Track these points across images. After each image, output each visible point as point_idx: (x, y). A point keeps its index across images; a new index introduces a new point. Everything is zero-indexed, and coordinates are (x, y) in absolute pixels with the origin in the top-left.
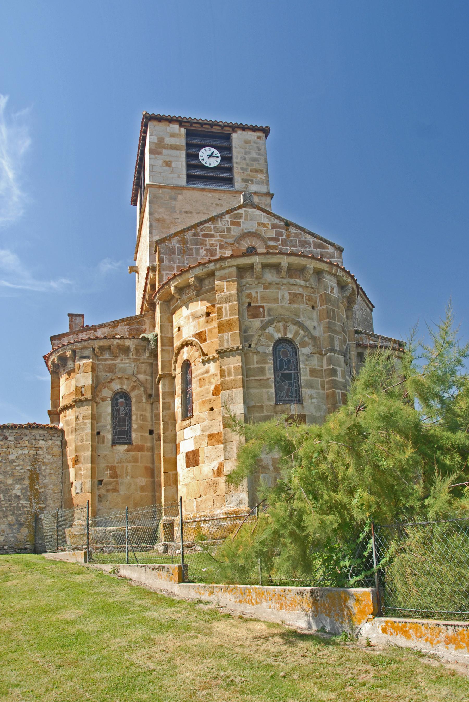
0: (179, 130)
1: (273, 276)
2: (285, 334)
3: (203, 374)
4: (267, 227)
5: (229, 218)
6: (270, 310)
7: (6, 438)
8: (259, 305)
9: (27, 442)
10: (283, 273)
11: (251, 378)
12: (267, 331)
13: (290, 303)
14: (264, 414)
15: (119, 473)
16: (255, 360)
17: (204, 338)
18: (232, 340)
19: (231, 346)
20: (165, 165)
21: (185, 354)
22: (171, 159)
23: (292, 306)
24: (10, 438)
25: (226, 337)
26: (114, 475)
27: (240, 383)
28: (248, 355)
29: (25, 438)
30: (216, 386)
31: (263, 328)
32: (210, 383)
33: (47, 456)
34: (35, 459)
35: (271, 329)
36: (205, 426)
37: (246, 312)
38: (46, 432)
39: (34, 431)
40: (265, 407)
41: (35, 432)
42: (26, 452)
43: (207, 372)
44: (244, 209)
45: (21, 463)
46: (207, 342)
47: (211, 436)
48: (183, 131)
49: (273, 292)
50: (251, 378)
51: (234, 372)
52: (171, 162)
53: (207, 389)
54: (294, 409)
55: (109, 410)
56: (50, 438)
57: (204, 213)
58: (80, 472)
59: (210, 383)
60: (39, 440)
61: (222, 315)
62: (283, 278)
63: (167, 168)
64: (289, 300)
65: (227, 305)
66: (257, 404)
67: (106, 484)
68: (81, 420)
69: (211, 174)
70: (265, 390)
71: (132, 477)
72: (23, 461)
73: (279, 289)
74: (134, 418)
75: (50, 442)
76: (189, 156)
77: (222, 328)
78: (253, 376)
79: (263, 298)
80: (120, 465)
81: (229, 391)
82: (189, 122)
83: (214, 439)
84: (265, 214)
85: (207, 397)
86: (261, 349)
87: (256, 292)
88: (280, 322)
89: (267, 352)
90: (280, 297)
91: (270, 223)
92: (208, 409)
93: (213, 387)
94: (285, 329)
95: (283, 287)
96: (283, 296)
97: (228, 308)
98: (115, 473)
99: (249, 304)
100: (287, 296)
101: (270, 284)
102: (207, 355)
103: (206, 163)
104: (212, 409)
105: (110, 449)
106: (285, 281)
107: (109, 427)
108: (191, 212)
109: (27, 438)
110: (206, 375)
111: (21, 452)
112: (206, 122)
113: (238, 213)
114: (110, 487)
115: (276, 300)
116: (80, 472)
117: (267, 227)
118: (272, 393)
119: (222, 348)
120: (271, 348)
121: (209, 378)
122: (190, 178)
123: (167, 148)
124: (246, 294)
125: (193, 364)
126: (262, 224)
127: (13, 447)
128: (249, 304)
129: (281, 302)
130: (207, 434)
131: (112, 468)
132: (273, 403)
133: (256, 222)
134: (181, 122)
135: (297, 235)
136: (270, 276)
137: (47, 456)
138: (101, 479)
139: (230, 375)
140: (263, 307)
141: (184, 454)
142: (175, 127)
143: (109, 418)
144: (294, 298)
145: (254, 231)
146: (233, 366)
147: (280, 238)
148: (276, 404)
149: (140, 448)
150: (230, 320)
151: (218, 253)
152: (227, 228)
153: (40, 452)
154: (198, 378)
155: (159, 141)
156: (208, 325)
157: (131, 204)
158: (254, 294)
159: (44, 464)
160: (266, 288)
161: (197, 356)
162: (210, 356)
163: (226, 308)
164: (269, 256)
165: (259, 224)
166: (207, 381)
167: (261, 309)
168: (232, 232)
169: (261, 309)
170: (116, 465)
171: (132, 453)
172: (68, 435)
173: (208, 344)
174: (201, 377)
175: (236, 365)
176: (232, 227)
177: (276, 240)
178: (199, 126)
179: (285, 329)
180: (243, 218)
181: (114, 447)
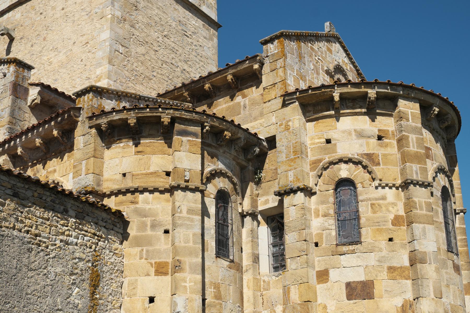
3: (376, 199)
18: (421, 174)
25: (414, 168)
30: (395, 216)
36: (383, 257)
38: (109, 217)
41: (97, 212)
43: (384, 198)
46: (381, 166)
47: (391, 269)
51: (426, 208)
62: (441, 128)
85: (384, 225)
93: (392, 217)
97: (415, 139)
104: (391, 240)
105: (214, 259)
110: (381, 202)
121: (386, 206)
125: (359, 186)
130: (386, 265)
131: (217, 287)
146: (424, 200)
150: (417, 152)
154: (370, 202)
156: (382, 149)
163: (412, 139)
166: (384, 208)
175: (426, 200)
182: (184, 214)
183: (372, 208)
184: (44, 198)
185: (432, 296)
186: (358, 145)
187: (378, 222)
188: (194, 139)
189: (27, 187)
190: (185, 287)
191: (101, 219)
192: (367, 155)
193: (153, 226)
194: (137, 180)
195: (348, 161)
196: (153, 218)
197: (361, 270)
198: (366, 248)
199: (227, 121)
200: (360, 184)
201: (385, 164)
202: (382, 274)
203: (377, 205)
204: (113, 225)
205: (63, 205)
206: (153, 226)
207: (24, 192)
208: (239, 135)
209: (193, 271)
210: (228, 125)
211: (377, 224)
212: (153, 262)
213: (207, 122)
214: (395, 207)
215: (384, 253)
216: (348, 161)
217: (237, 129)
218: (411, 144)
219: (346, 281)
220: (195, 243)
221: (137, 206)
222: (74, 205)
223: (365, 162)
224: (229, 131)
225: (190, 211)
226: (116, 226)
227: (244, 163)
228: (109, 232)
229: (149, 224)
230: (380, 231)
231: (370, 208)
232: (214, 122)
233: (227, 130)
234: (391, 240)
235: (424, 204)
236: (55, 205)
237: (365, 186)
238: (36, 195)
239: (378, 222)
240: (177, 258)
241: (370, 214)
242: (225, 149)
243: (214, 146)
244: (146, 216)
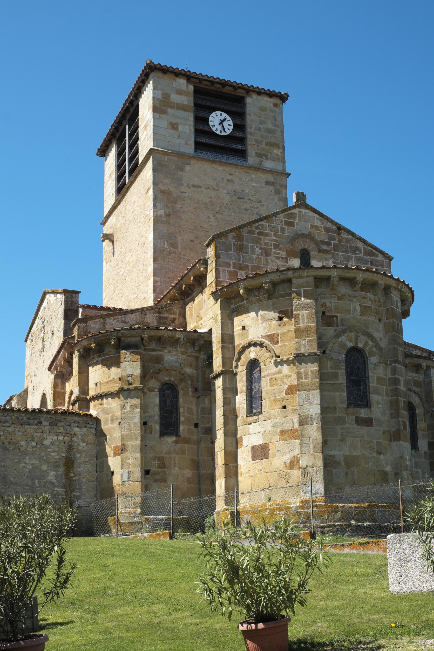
0: (187, 86)
1: (346, 289)
2: (357, 343)
3: (274, 374)
4: (319, 230)
5: (284, 218)
6: (343, 320)
7: (41, 423)
8: (333, 314)
9: (62, 428)
10: (358, 287)
11: (324, 382)
12: (340, 339)
13: (361, 315)
14: (337, 415)
15: (167, 464)
16: (329, 366)
17: (276, 340)
19: (308, 351)
20: (170, 127)
21: (252, 353)
22: (178, 121)
23: (363, 318)
24: (45, 423)
25: (303, 342)
26: (162, 466)
27: (317, 385)
28: (322, 360)
29: (60, 424)
30: (289, 386)
31: (337, 336)
32: (283, 383)
33: (81, 444)
34: (70, 447)
35: (343, 338)
36: (277, 423)
37: (321, 320)
38: (81, 419)
39: (68, 417)
40: (337, 409)
41: (69, 418)
42: (61, 438)
44: (298, 209)
45: (56, 449)
46: (280, 344)
47: (283, 432)
48: (191, 87)
49: (345, 304)
50: (324, 382)
51: (311, 376)
52: (177, 124)
53: (280, 389)
54: (363, 413)
55: (157, 400)
56: (84, 425)
57: (214, 189)
58: (127, 461)
59: (283, 383)
60: (74, 427)
61: (299, 322)
63: (174, 131)
64: (360, 312)
65: (305, 313)
66: (330, 406)
67: (154, 474)
68: (128, 409)
69: (221, 144)
70: (337, 393)
71: (180, 469)
72: (58, 448)
73: (351, 301)
74: (181, 410)
75: (85, 429)
76: (197, 119)
77: (299, 333)
78: (327, 380)
79: (337, 309)
80: (168, 456)
81: (306, 392)
82: (199, 79)
83: (287, 435)
84: (318, 216)
85: (279, 395)
86: (334, 356)
87: (331, 302)
88: (352, 332)
89: (340, 358)
90: (352, 309)
91: (323, 226)
92: (281, 406)
93: (286, 387)
94: (357, 339)
95: (355, 300)
96: (355, 308)
97: (305, 315)
98: (164, 463)
99: (324, 313)
100: (358, 308)
101: (343, 295)
102: (279, 357)
103: (217, 130)
104: (285, 407)
106: (357, 294)
107: (157, 418)
108: (199, 187)
109: (62, 424)
110: (277, 376)
111: (55, 438)
112: (218, 80)
113: (292, 213)
114: (158, 477)
115: (348, 311)
116: (127, 461)
117: (319, 230)
118: (344, 397)
119: (300, 352)
120: (344, 356)
121: (282, 379)
122: (198, 145)
123: (172, 107)
124: (321, 303)
125: (262, 364)
126: (315, 226)
127: (48, 432)
128: (324, 313)
129: (353, 314)
131: (161, 459)
132: (345, 405)
133: (310, 224)
134: (189, 77)
135: (348, 241)
136: (344, 289)
137: (81, 444)
138: (148, 468)
139: (307, 377)
140: (337, 317)
141: (250, 449)
142: (182, 82)
143: (157, 409)
144: (365, 310)
145: (307, 233)
146: (310, 369)
147: (333, 242)
148: (348, 407)
149: (187, 441)
150: (307, 327)
151: (272, 252)
152: (281, 228)
153: (75, 439)
154: (269, 377)
155: (163, 97)
156: (281, 328)
157: (97, 154)
158: (328, 304)
159: (79, 451)
160: (339, 299)
161: (267, 357)
162: (284, 357)
164: (348, 270)
165: (312, 226)
166: (279, 381)
167: (335, 319)
168: (286, 232)
169: (335, 319)
170: (164, 456)
171: (180, 445)
172: (106, 423)
173: (281, 346)
174: (273, 377)
175: (313, 369)
176: (286, 227)
177: (328, 244)
178: (209, 83)
179: (357, 339)
180: (297, 218)
181: (162, 438)
182: (128, 409)
183: (270, 382)
184: (20, 418)
185: (312, 452)
186: (262, 329)
187: (274, 394)
189: (6, 414)
190: (129, 463)
191: (73, 422)
192: (269, 336)
193: (112, 420)
194: (103, 387)
195: (255, 344)
196: (112, 415)
197: (260, 435)
198: (265, 417)
200: (263, 363)
201: (282, 342)
202: (275, 438)
203: (274, 379)
204: (86, 423)
205: (36, 419)
206: (112, 420)
207: (4, 418)
208: (177, 336)
209: (134, 451)
211: (273, 395)
212: (112, 446)
214: (289, 378)
215: (278, 419)
216: (255, 344)
217: (174, 332)
218: (301, 321)
219: (251, 446)
220: (135, 430)
221: (103, 406)
222: (47, 417)
223: (267, 342)
225: (132, 406)
226: (89, 424)
227: (197, 355)
228: (81, 430)
229: (110, 419)
230: (275, 401)
231: (269, 382)
234: (285, 407)
235: (310, 372)
236: (30, 421)
237: (267, 363)
238: (13, 417)
239: (274, 394)
240: (123, 443)
241: (269, 388)
242: (171, 349)
243: (158, 350)
244: (108, 414)
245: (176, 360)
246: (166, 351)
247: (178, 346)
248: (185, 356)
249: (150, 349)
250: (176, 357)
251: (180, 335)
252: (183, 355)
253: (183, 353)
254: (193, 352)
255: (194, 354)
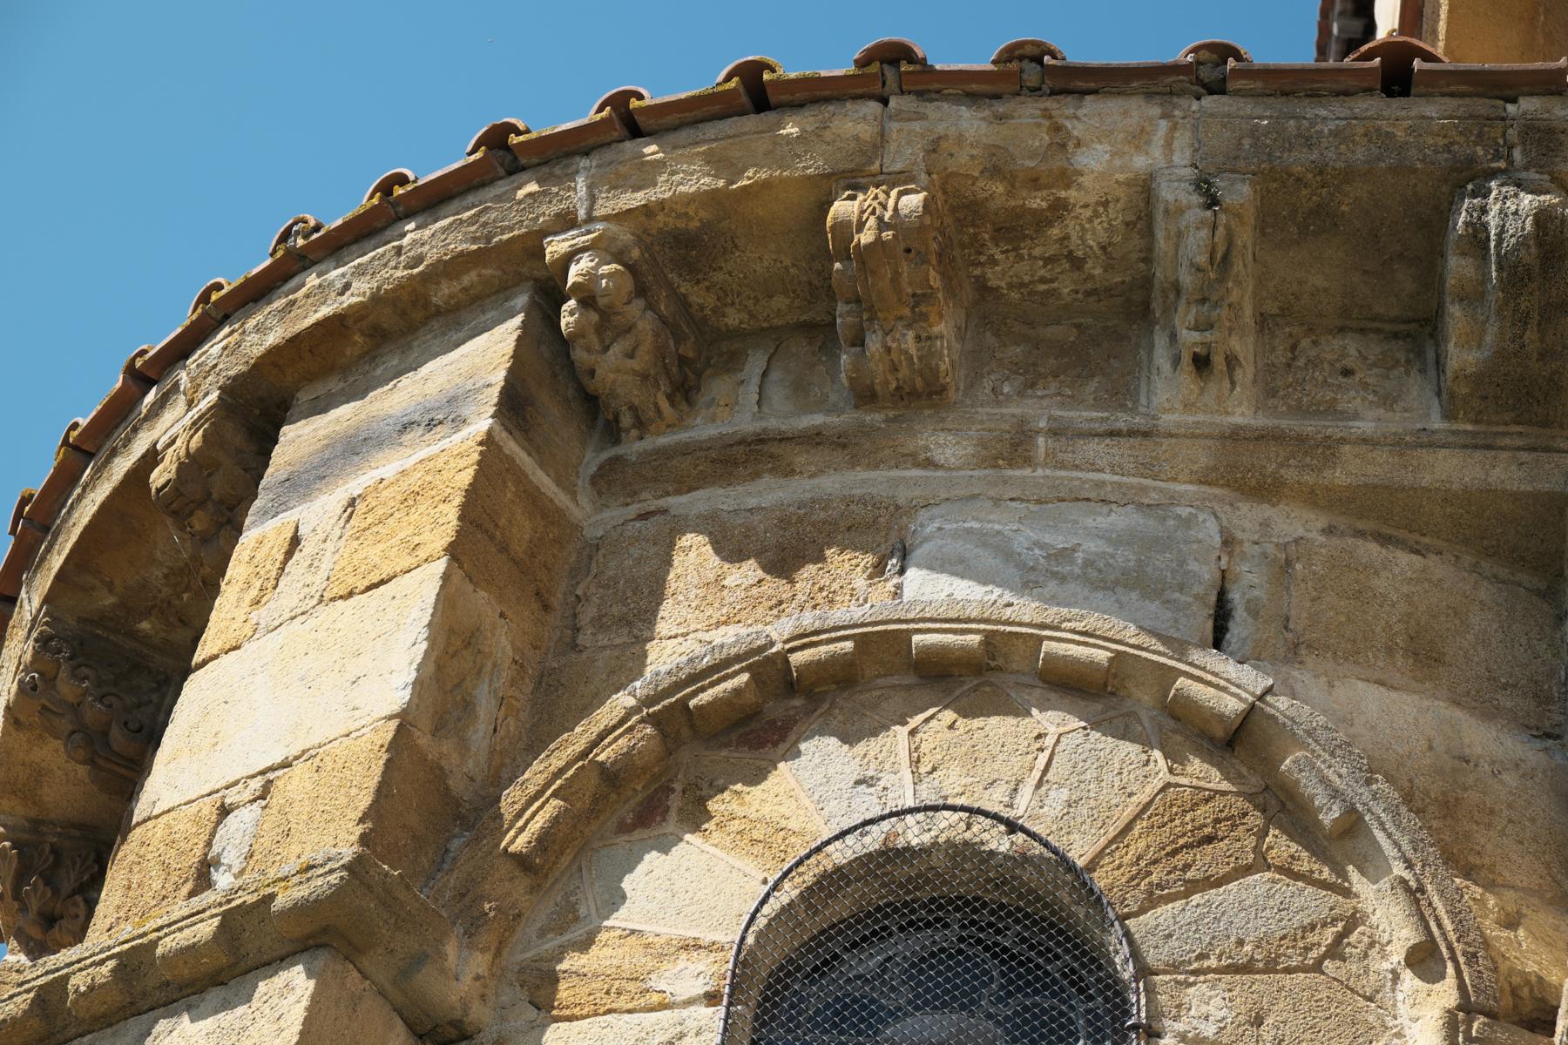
188: (423, 453)
199: (815, 94)
210: (855, 122)
213: (567, 221)
217: (1027, 112)
224: (900, 180)
232: (646, 175)
233: (854, 182)
242: (1039, 410)
243: (814, 439)
245: (1125, 557)
246: (948, 446)
247: (1162, 357)
248: (1293, 523)
249: (685, 450)
250: (1120, 519)
251: (1139, 138)
252: (1265, 490)
253: (1243, 471)
254: (1427, 441)
255: (1451, 469)
